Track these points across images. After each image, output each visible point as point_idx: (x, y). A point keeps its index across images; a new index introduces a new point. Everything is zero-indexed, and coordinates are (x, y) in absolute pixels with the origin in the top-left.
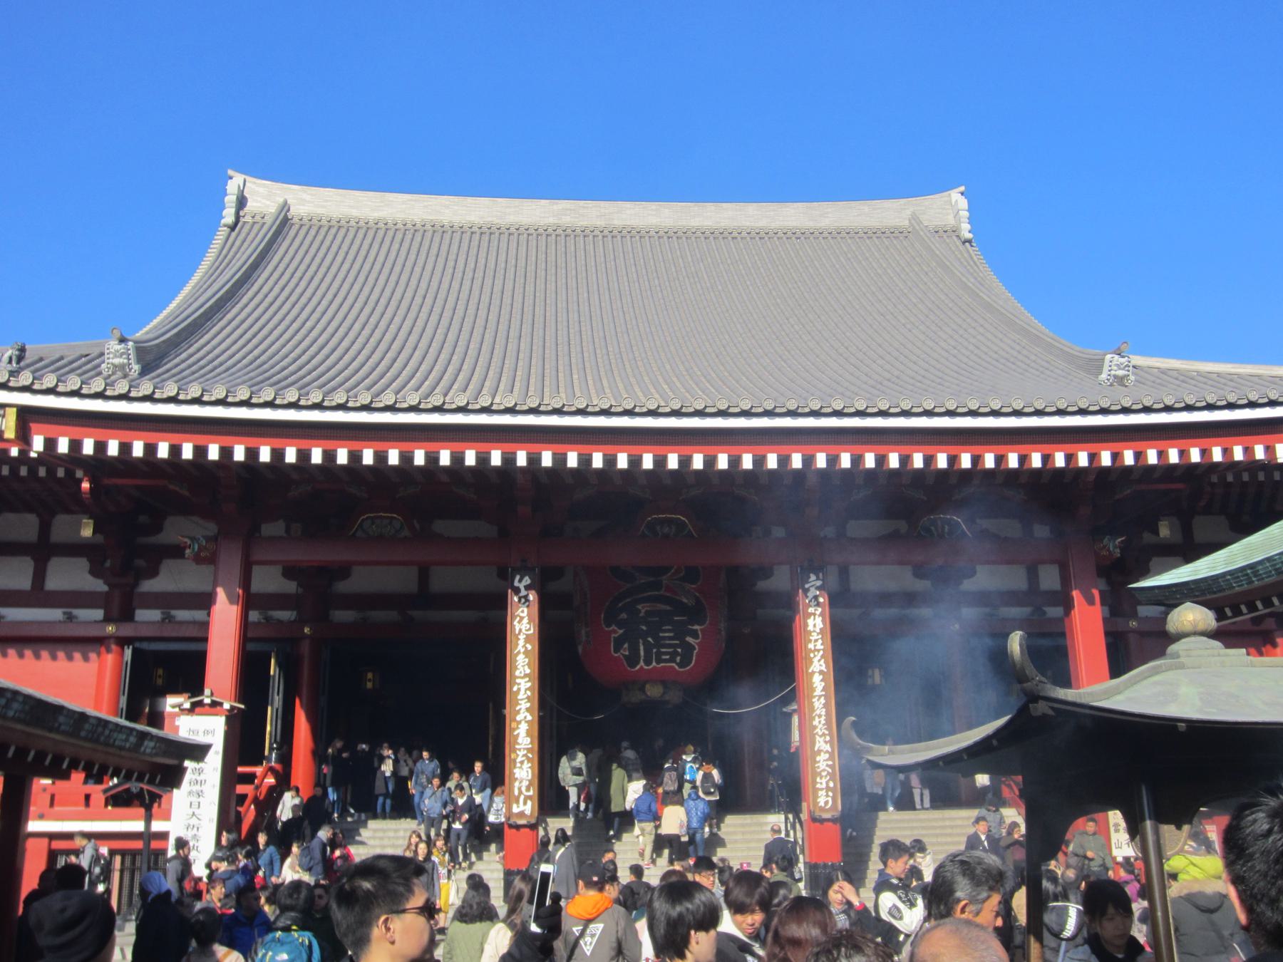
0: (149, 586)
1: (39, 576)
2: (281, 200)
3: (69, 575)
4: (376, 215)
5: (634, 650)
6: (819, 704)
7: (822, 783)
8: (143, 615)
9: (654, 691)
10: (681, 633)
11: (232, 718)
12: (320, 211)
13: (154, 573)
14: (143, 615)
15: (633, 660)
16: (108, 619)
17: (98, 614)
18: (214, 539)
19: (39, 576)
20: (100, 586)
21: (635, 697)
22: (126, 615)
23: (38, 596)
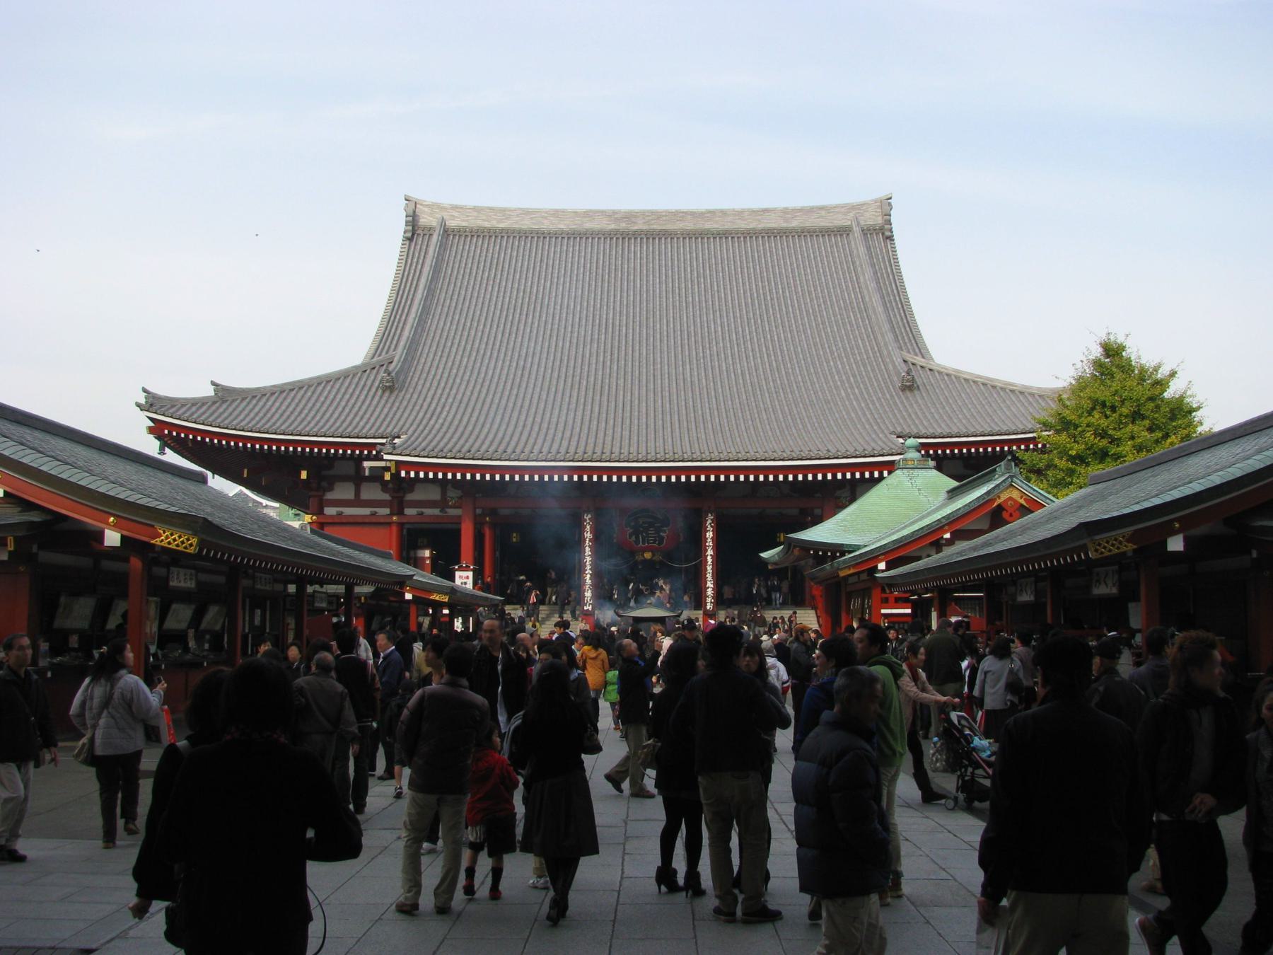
0: (409, 497)
1: (357, 493)
2: (439, 216)
3: (371, 492)
4: (501, 225)
5: (637, 538)
6: (709, 568)
7: (709, 600)
8: (410, 511)
9: (648, 555)
10: (658, 531)
11: (474, 570)
12: (464, 224)
13: (412, 491)
14: (410, 511)
15: (637, 541)
16: (392, 514)
17: (387, 511)
18: (460, 498)
19: (357, 493)
20: (387, 497)
21: (639, 558)
22: (400, 512)
23: (358, 502)
